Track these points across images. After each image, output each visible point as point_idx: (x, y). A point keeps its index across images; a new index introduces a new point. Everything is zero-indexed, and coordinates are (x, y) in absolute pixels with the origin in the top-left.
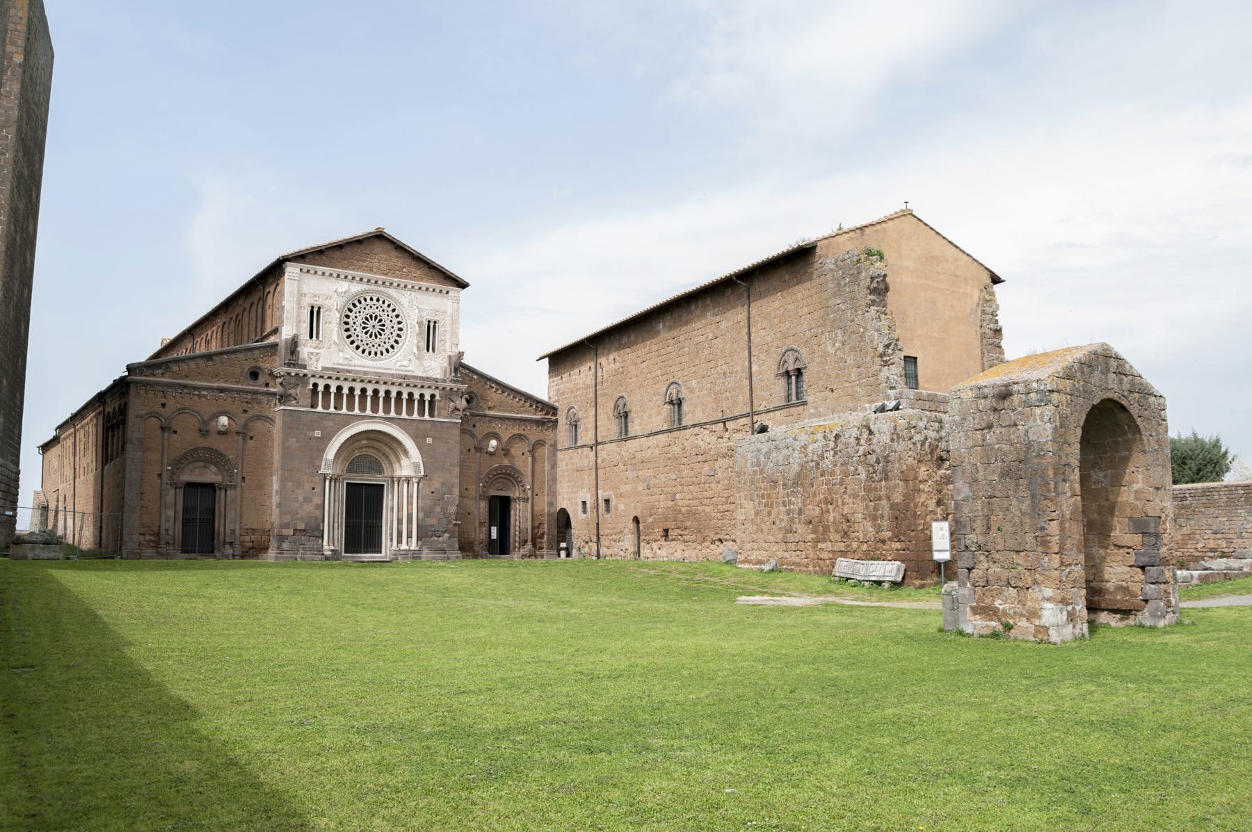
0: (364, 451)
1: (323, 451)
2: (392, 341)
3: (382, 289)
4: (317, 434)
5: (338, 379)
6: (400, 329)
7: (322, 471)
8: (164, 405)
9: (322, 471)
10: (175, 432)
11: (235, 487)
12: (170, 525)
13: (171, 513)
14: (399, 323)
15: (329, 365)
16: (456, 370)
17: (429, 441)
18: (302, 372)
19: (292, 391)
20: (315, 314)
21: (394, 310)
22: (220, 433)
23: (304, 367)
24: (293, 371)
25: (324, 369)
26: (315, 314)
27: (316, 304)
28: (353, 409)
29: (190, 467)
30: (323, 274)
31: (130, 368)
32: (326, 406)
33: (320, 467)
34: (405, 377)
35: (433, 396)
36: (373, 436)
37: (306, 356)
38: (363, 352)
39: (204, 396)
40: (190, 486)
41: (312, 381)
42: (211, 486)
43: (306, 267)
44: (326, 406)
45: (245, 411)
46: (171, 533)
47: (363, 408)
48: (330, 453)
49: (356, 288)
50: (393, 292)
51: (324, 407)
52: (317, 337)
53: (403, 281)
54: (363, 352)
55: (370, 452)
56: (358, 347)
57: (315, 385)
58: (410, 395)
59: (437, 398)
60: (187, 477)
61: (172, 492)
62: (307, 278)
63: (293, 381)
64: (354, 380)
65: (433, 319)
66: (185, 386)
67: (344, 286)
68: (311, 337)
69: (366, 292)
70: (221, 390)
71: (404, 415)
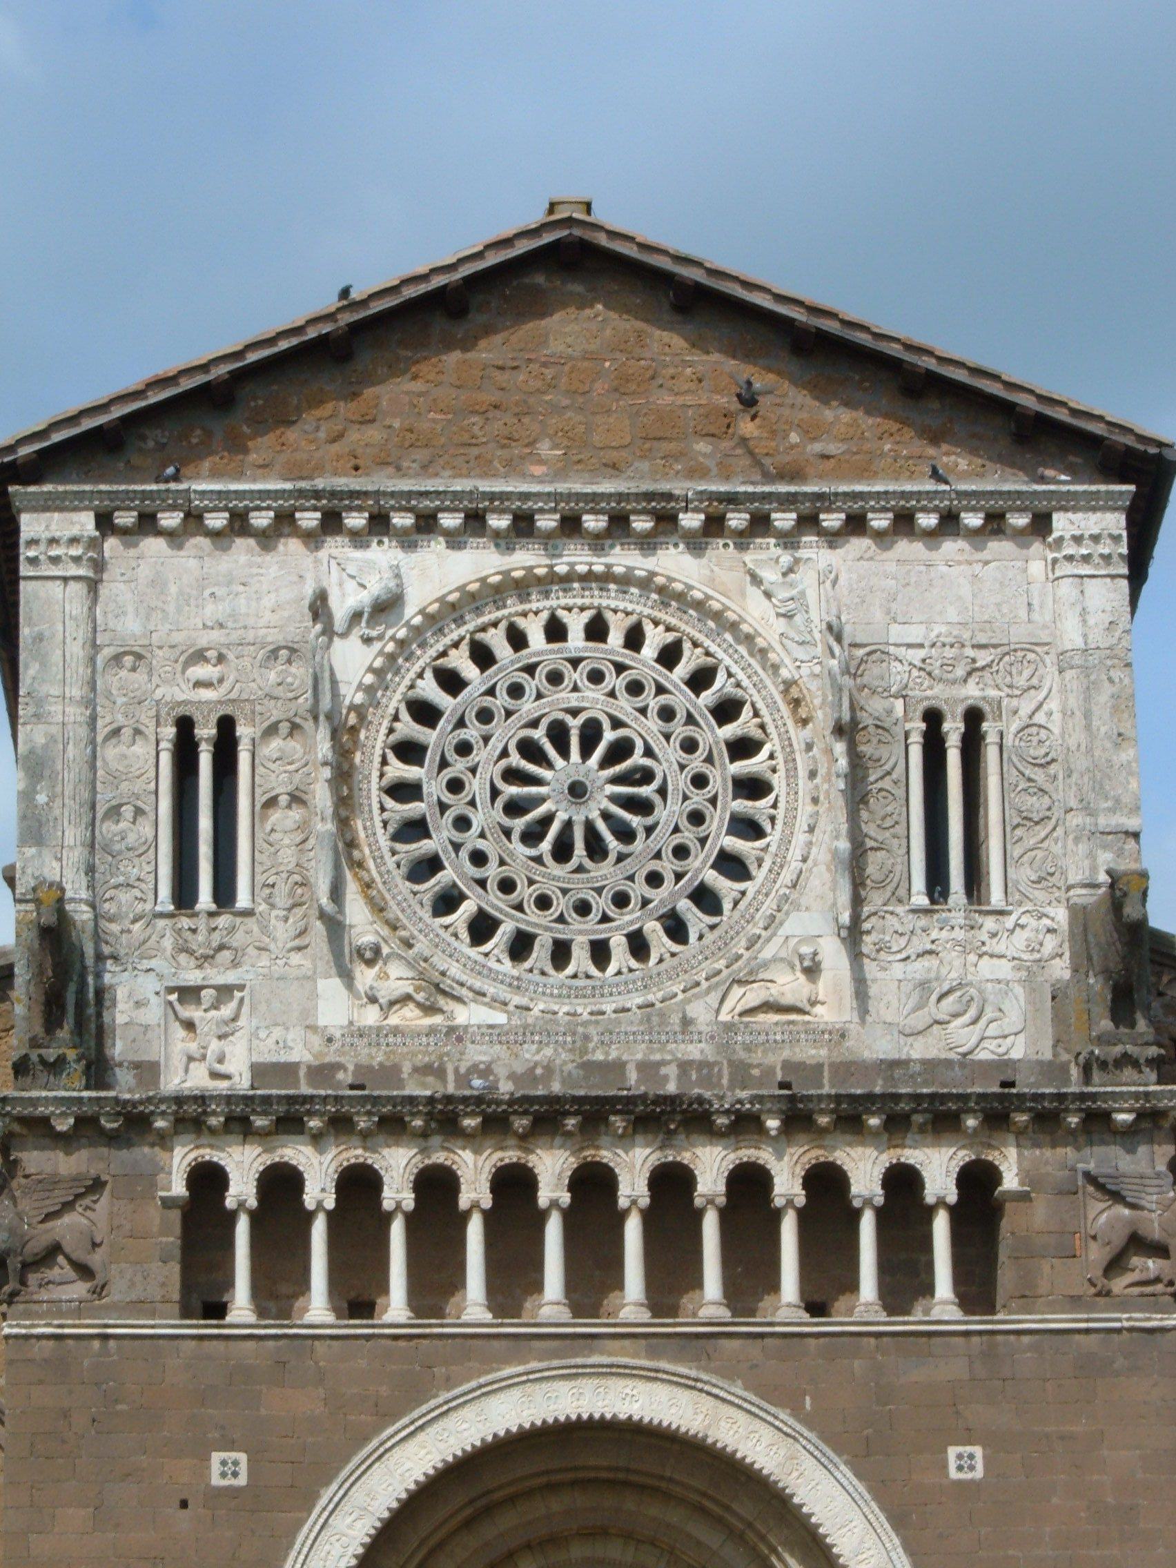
4: (227, 1468)
6: (753, 787)
14: (742, 748)
16: (1123, 1003)
17: (965, 1462)
19: (68, 1228)
20: (205, 757)
21: (700, 680)
26: (205, 757)
27: (207, 704)
35: (977, 1181)
56: (482, 928)
57: (208, 1179)
58: (826, 1183)
59: (1010, 1181)
65: (955, 698)
67: (356, 572)
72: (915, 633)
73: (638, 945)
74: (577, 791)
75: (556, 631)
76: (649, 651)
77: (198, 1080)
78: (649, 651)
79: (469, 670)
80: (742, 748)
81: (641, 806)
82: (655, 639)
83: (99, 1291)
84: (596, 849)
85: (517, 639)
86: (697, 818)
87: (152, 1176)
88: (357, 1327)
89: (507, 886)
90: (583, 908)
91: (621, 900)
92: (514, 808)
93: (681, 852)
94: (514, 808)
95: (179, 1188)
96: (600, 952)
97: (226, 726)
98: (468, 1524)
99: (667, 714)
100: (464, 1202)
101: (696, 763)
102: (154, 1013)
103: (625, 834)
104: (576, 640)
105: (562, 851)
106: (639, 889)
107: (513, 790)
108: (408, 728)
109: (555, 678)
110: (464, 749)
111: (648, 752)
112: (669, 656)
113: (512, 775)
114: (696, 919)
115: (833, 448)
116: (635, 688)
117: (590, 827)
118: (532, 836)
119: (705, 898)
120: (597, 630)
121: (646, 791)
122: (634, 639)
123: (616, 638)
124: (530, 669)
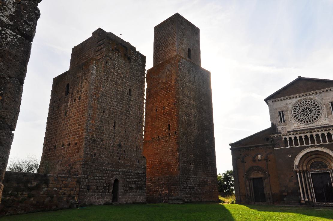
0: (316, 160)
1: (293, 162)
2: (316, 115)
3: (307, 97)
4: (290, 156)
5: (293, 134)
6: (319, 109)
7: (294, 169)
8: (241, 154)
9: (294, 169)
10: (246, 162)
11: (267, 178)
12: (249, 192)
13: (248, 188)
15: (290, 130)
18: (278, 135)
20: (281, 113)
21: (314, 103)
22: (259, 160)
23: (281, 133)
24: (275, 136)
25: (288, 132)
26: (281, 113)
28: (303, 144)
29: (253, 173)
30: (281, 100)
31: (231, 145)
32: (291, 145)
33: (293, 168)
34: (325, 127)
36: (315, 153)
37: (281, 129)
38: (304, 122)
39: (252, 149)
40: (254, 179)
41: (284, 137)
42: (261, 178)
43: (274, 100)
44: (291, 145)
45: (265, 152)
46: (249, 195)
47: (307, 143)
48: (296, 162)
49: (294, 100)
50: (311, 97)
51: (290, 146)
52: (284, 121)
53: (314, 92)
54: (304, 122)
55: (319, 160)
56: (301, 121)
57: (285, 139)
60: (252, 176)
61: (248, 182)
62: (277, 103)
63: (276, 139)
64: (300, 133)
66: (246, 148)
67: (289, 101)
68: (281, 122)
69: (299, 101)
70: (256, 147)
71: (328, 143)
72: (329, 97)
73: (313, 121)
74: (307, 112)
75: (303, 102)
76: (310, 102)
77: (284, 133)
78: (310, 102)
79: (298, 106)
80: (318, 107)
81: (311, 112)
82: (310, 102)
83: (280, 146)
84: (309, 115)
85: (301, 103)
86: (315, 112)
87: (282, 138)
88: (297, 146)
89: (303, 118)
90: (308, 119)
91: (311, 118)
92: (302, 113)
93: (315, 114)
94: (302, 113)
95: (283, 139)
96: (310, 121)
97: (282, 112)
98: (307, 158)
99: (312, 106)
100: (303, 138)
101: (315, 108)
102: (281, 129)
103: (310, 114)
104: (305, 103)
105: (306, 115)
106: (312, 117)
107: (302, 112)
108: (294, 110)
109: (304, 105)
110: (298, 110)
111: (311, 108)
112: (312, 102)
113: (302, 112)
114: (316, 118)
115: (321, 87)
116: (309, 105)
117: (308, 114)
118: (304, 115)
119: (317, 117)
120: (306, 102)
121: (312, 111)
122: (309, 102)
123: (308, 102)
124: (302, 105)
